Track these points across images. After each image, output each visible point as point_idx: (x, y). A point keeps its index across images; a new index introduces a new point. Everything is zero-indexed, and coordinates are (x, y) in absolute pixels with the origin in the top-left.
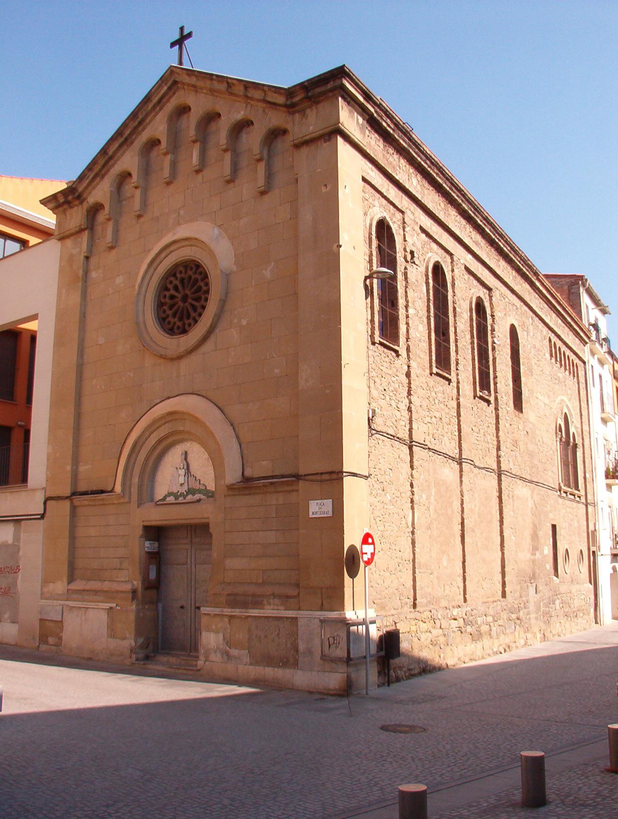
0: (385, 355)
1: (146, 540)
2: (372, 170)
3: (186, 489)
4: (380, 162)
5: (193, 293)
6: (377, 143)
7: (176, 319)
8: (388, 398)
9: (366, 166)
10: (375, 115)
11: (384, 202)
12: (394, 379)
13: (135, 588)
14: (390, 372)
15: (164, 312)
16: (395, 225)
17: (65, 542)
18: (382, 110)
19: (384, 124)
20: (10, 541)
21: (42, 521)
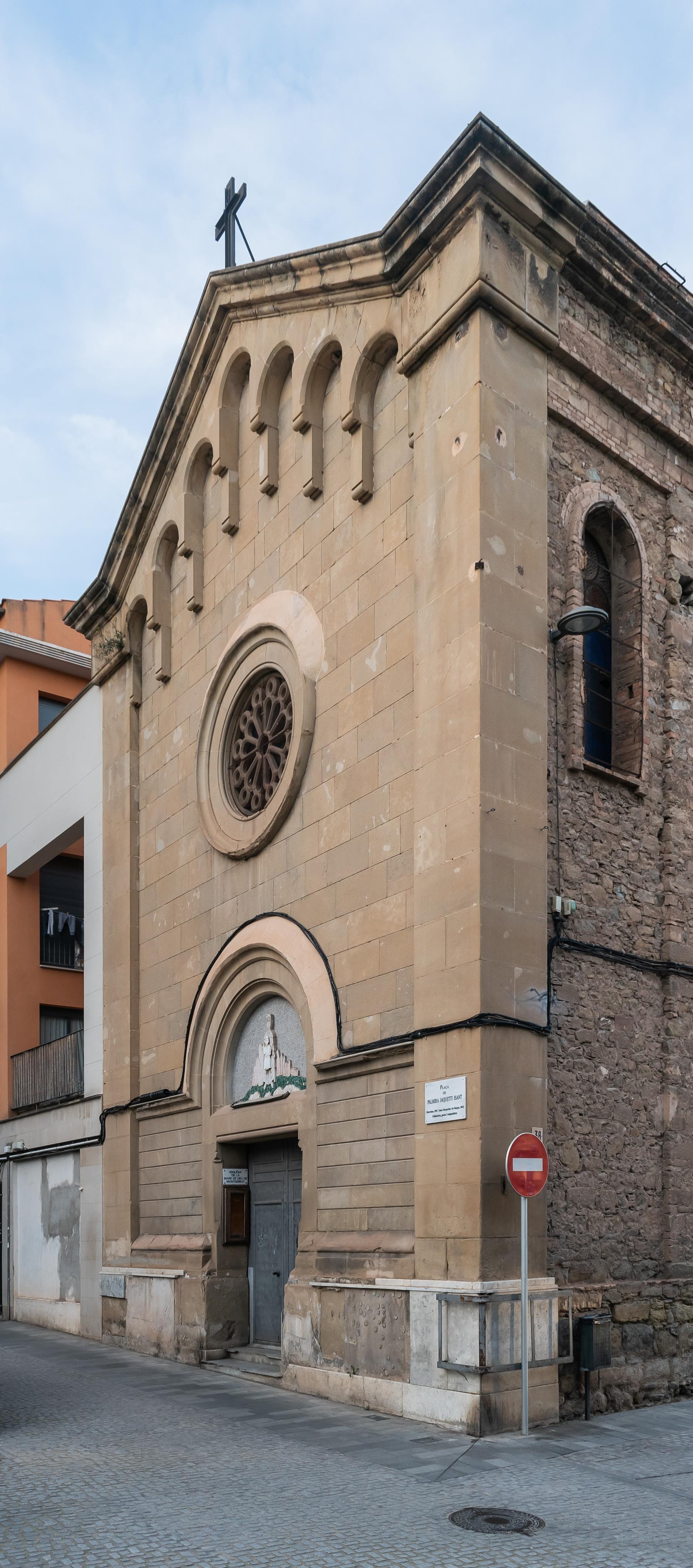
0: (603, 796)
1: (223, 1168)
2: (580, 397)
3: (274, 1078)
4: (599, 374)
5: (273, 734)
6: (592, 328)
7: (254, 786)
8: (608, 881)
9: (563, 386)
10: (579, 251)
11: (615, 471)
12: (625, 844)
13: (209, 1244)
14: (617, 830)
15: (238, 775)
16: (645, 524)
17: (126, 1177)
18: (597, 238)
19: (605, 273)
20: (71, 1182)
21: (100, 1147)
